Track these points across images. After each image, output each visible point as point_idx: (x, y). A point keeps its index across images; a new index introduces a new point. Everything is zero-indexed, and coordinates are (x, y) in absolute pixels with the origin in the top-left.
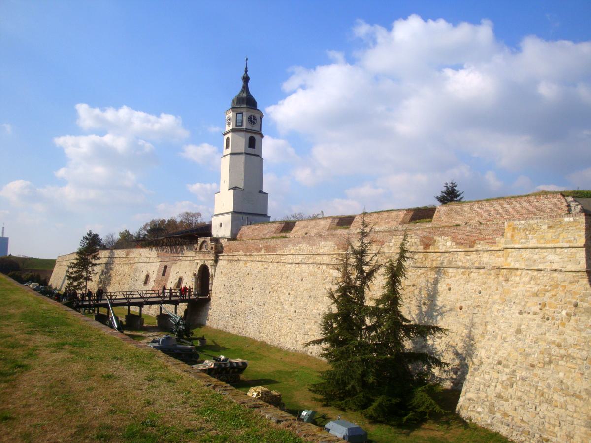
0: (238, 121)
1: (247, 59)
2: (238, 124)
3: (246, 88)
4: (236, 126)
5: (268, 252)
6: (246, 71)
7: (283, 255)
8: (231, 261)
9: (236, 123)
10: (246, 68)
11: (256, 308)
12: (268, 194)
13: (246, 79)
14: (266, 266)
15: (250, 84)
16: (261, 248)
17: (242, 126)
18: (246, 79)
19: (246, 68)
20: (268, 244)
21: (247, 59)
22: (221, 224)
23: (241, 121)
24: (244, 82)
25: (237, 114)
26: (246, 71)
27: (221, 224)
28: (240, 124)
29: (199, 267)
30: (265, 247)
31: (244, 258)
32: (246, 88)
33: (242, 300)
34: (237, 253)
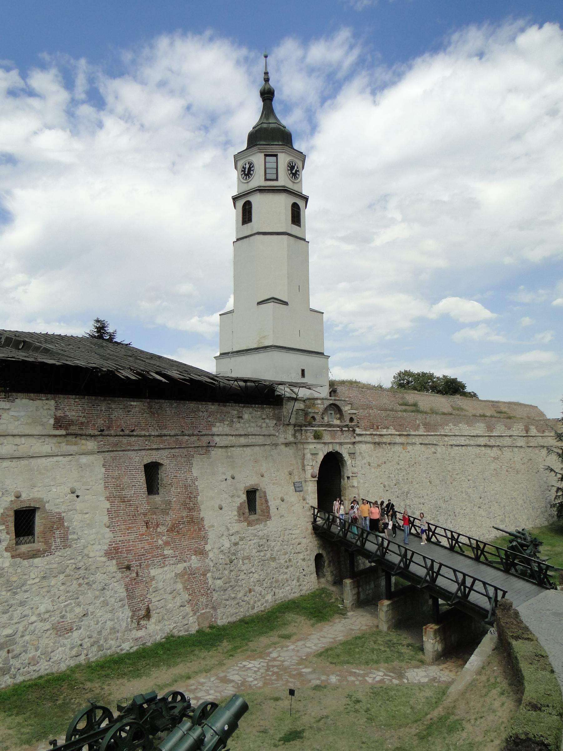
5: (428, 431)
6: (267, 80)
7: (446, 436)
8: (379, 444)
10: (266, 73)
11: (443, 505)
14: (433, 450)
16: (419, 426)
19: (266, 73)
20: (427, 421)
22: (303, 371)
26: (267, 80)
27: (303, 371)
29: (321, 457)
30: (424, 425)
31: (398, 440)
32: (268, 110)
33: (423, 501)
34: (385, 430)
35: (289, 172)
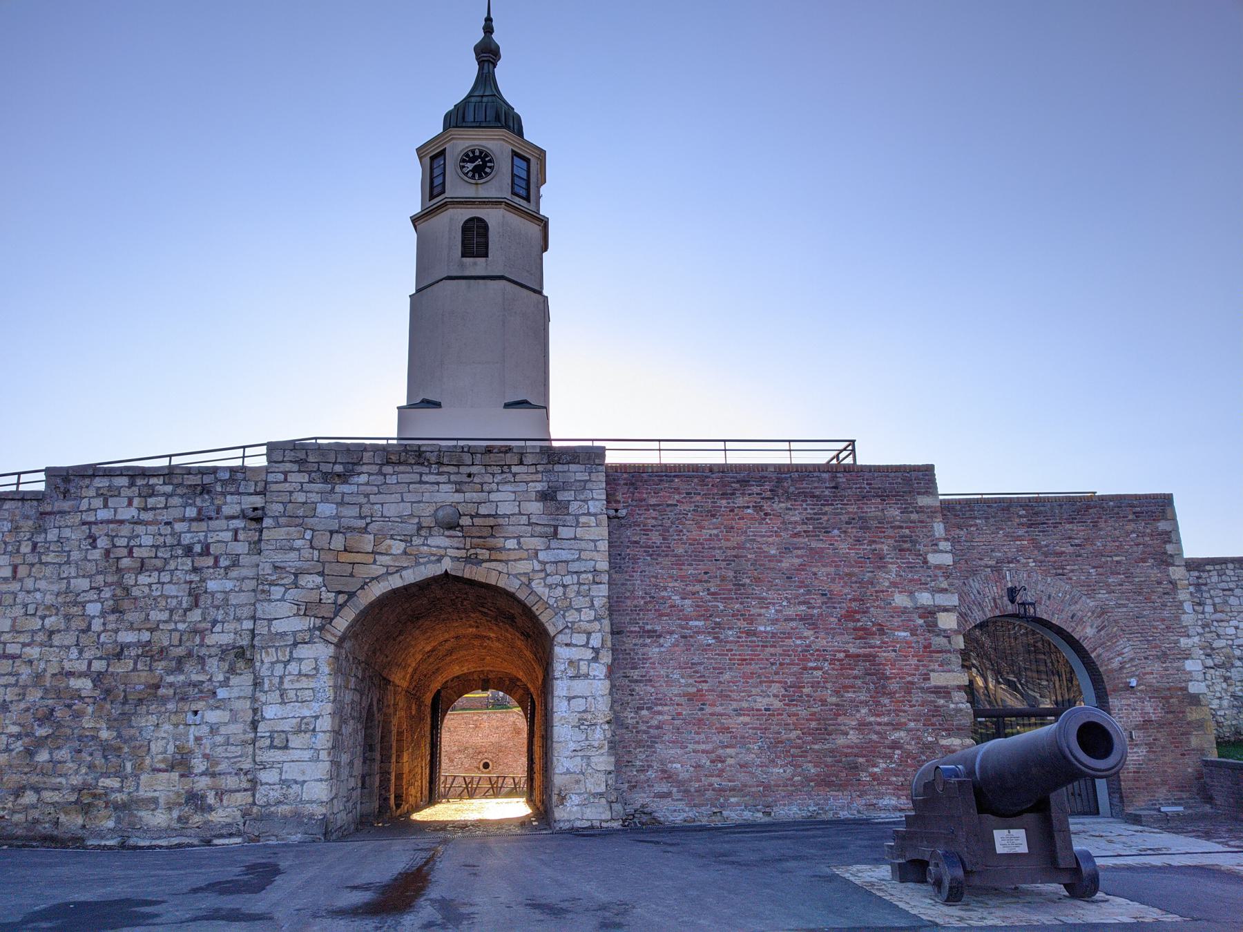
2: (517, 189)
3: (486, 78)
4: (514, 193)
6: (488, 29)
10: (489, 20)
13: (487, 54)
15: (503, 73)
17: (528, 199)
18: (487, 54)
19: (489, 20)
23: (523, 184)
24: (481, 63)
25: (515, 154)
26: (488, 29)
32: (486, 78)
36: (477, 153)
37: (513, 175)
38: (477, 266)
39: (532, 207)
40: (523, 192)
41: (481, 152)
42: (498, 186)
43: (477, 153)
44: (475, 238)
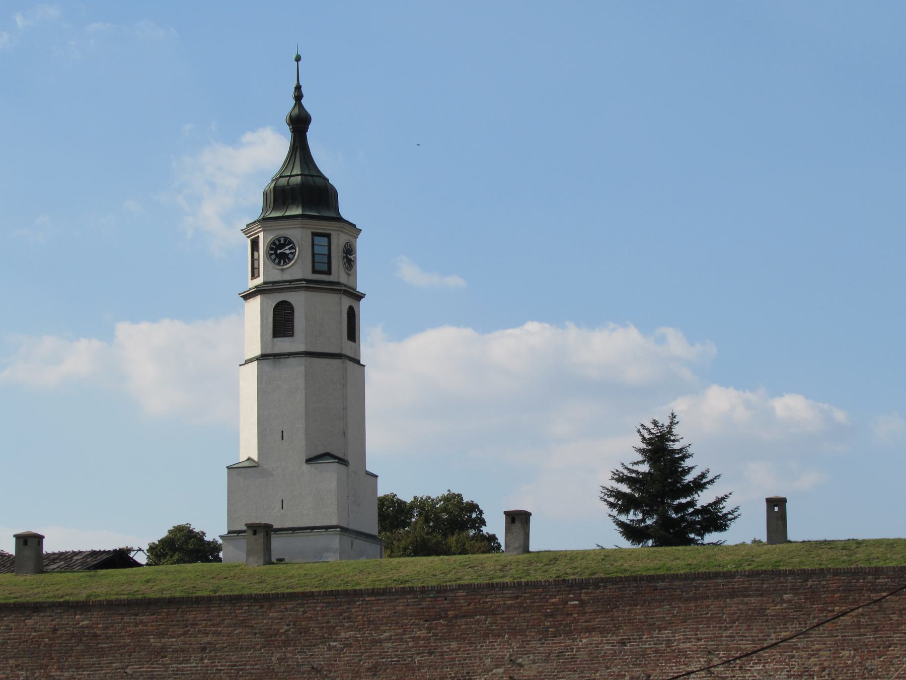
0: (317, 259)
1: (298, 59)
4: (314, 271)
6: (298, 97)
9: (313, 262)
10: (298, 88)
12: (377, 476)
13: (299, 123)
17: (329, 272)
18: (299, 123)
19: (298, 88)
21: (298, 59)
23: (325, 259)
25: (314, 234)
26: (298, 97)
28: (325, 268)
32: (300, 147)
35: (273, 257)
36: (282, 241)
37: (313, 255)
38: (284, 345)
39: (338, 274)
40: (325, 268)
41: (285, 240)
42: (299, 269)
43: (282, 241)
44: (281, 322)
